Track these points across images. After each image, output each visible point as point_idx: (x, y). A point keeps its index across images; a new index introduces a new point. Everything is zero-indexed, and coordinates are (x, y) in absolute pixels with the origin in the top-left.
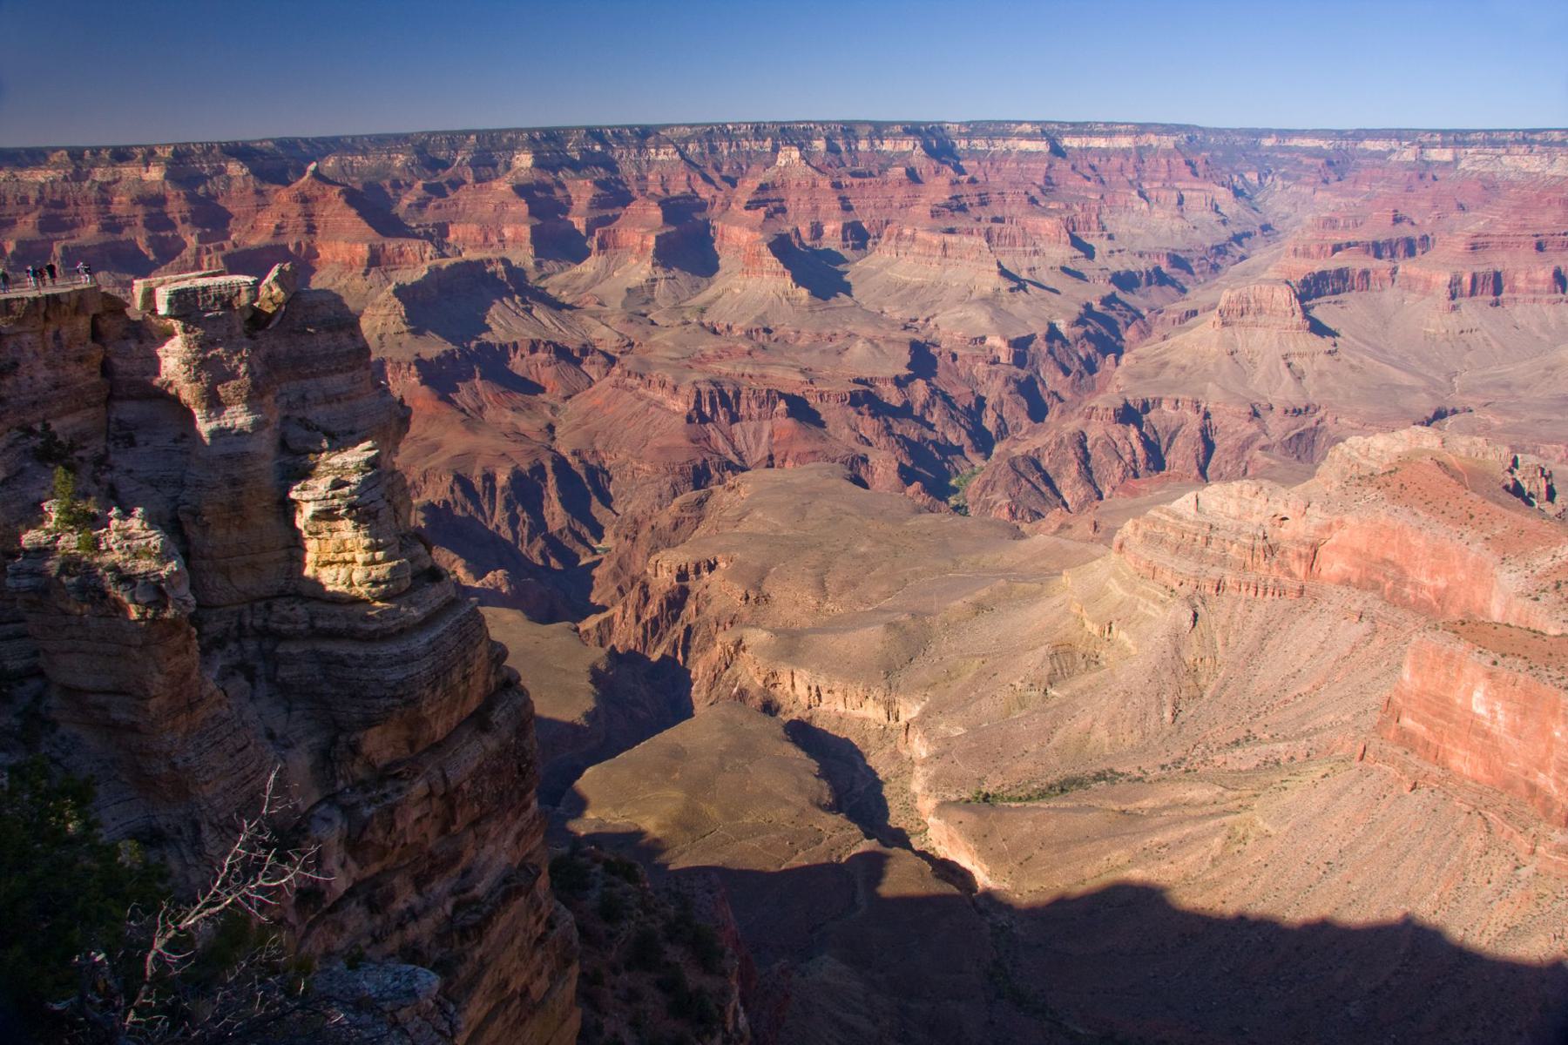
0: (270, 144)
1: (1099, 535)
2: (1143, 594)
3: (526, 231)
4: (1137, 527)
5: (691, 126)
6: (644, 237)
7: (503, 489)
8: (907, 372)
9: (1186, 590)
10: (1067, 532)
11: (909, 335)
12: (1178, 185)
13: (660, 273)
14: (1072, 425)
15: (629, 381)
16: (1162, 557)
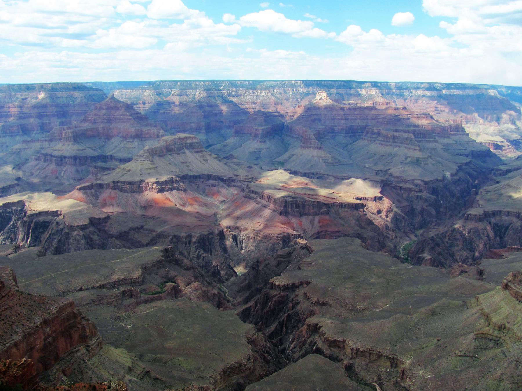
0: (91, 84)
1: (484, 277)
3: (203, 124)
7: (195, 243)
8: (380, 195)
13: (263, 146)
15: (252, 195)
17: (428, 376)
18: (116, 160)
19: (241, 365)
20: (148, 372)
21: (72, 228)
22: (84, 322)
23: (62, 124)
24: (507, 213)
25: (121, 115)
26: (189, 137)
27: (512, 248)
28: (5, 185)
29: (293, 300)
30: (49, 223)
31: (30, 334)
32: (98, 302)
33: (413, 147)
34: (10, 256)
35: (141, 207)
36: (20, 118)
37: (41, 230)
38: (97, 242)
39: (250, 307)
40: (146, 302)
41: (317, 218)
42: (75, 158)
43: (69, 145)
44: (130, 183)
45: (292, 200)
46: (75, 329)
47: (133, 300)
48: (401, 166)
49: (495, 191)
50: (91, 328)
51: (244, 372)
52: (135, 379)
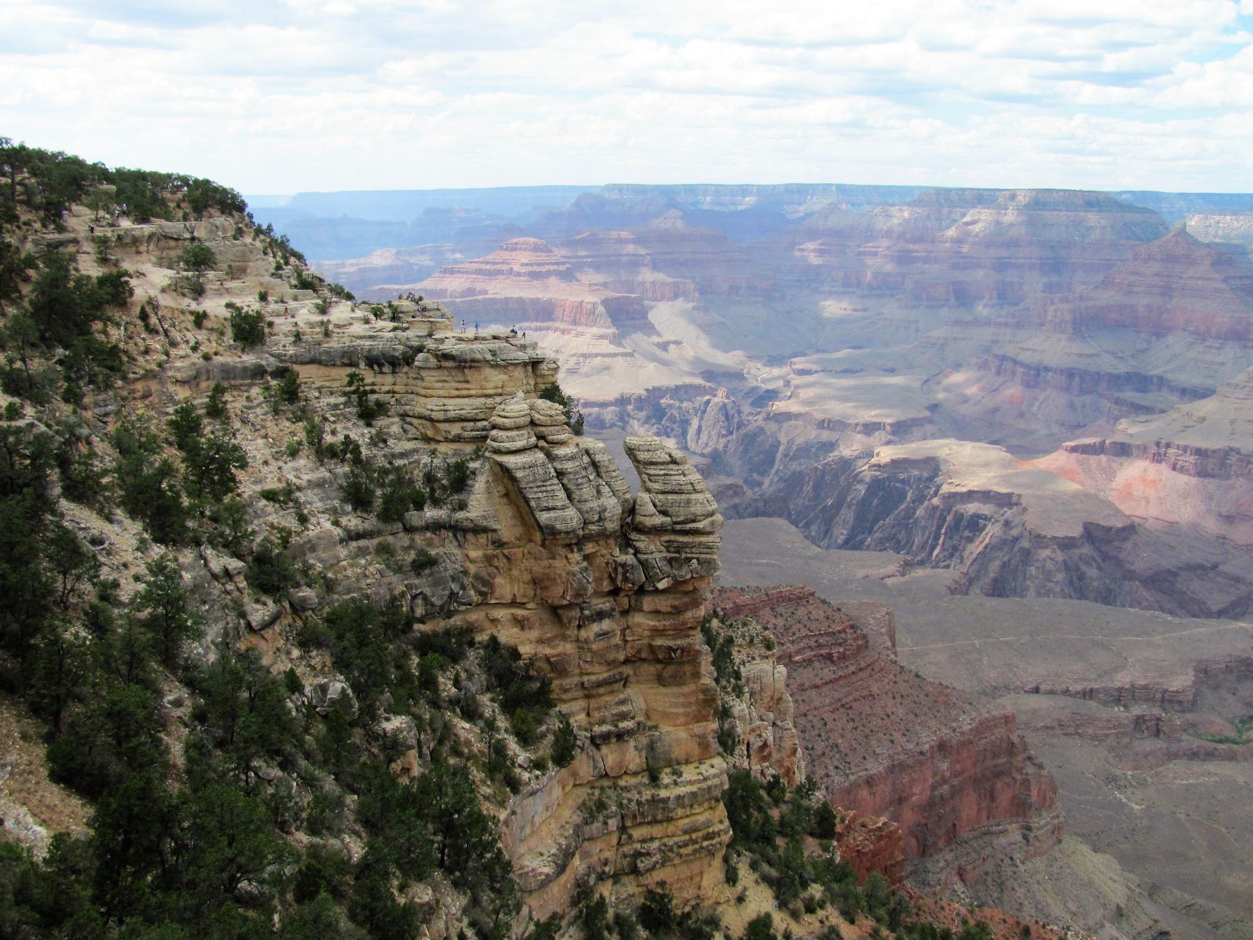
18: (1172, 389)
21: (1039, 540)
22: (1030, 769)
23: (1049, 288)
25: (1199, 278)
28: (903, 418)
30: (986, 518)
31: (902, 767)
32: (1071, 730)
34: (889, 581)
35: (1220, 515)
36: (955, 267)
37: (967, 533)
38: (1095, 584)
40: (1193, 755)
42: (1070, 373)
43: (1059, 340)
46: (1007, 780)
47: (1159, 744)
50: (1043, 787)
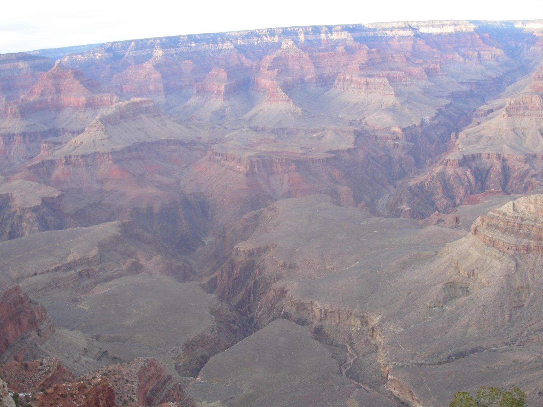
0: (38, 53)
1: (460, 224)
2: (489, 254)
3: (161, 86)
4: (483, 220)
5: (238, 32)
6: (219, 87)
8: (353, 147)
9: (511, 252)
10: (442, 224)
11: (352, 128)
12: (476, 48)
13: (227, 103)
14: (438, 169)
15: (216, 158)
16: (497, 235)
17: (399, 330)
19: (204, 337)
20: (105, 352)
22: (32, 306)
24: (487, 156)
26: (145, 101)
27: (490, 192)
29: (259, 266)
33: (388, 92)
39: (216, 277)
40: (106, 280)
41: (286, 177)
42: (24, 135)
44: (83, 156)
45: (258, 159)
47: (91, 280)
48: (376, 114)
49: (475, 133)
51: (208, 344)
52: (92, 360)
